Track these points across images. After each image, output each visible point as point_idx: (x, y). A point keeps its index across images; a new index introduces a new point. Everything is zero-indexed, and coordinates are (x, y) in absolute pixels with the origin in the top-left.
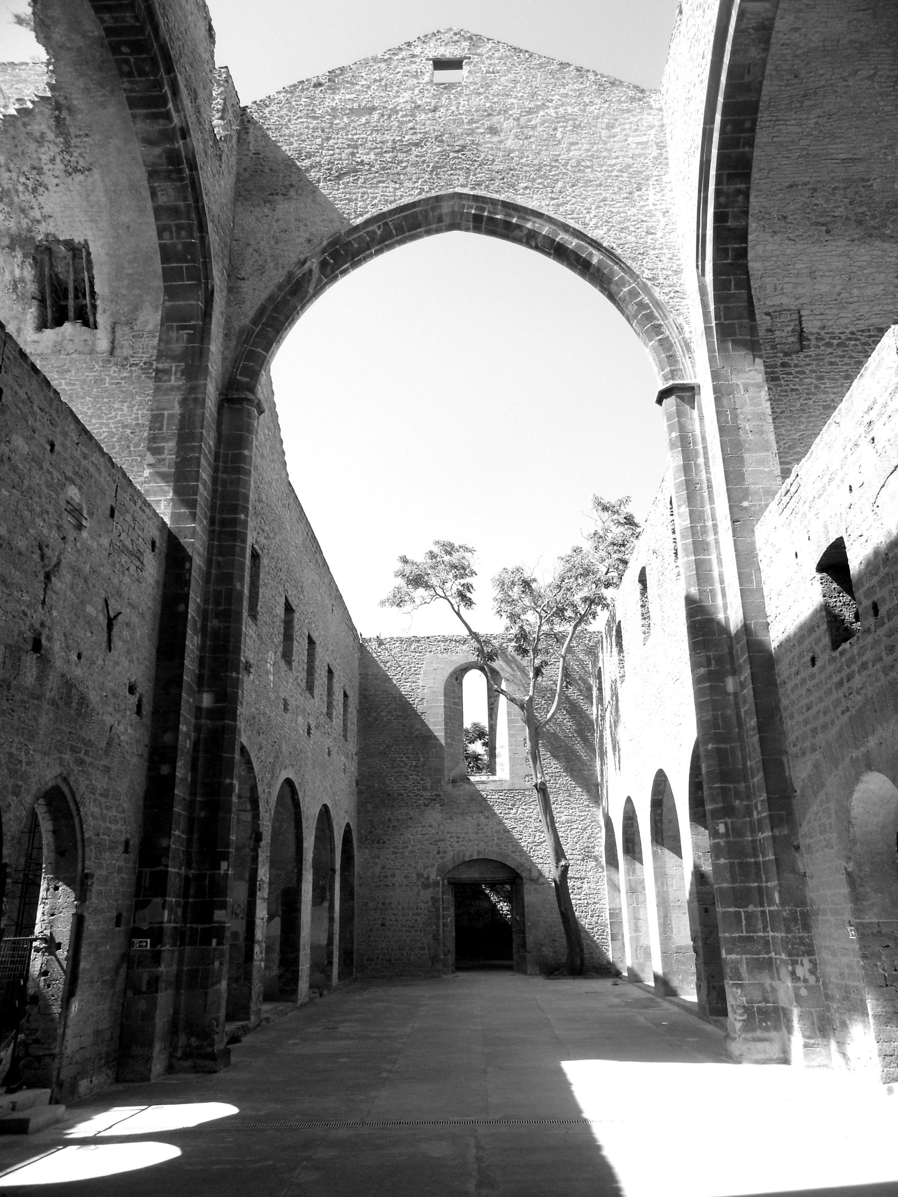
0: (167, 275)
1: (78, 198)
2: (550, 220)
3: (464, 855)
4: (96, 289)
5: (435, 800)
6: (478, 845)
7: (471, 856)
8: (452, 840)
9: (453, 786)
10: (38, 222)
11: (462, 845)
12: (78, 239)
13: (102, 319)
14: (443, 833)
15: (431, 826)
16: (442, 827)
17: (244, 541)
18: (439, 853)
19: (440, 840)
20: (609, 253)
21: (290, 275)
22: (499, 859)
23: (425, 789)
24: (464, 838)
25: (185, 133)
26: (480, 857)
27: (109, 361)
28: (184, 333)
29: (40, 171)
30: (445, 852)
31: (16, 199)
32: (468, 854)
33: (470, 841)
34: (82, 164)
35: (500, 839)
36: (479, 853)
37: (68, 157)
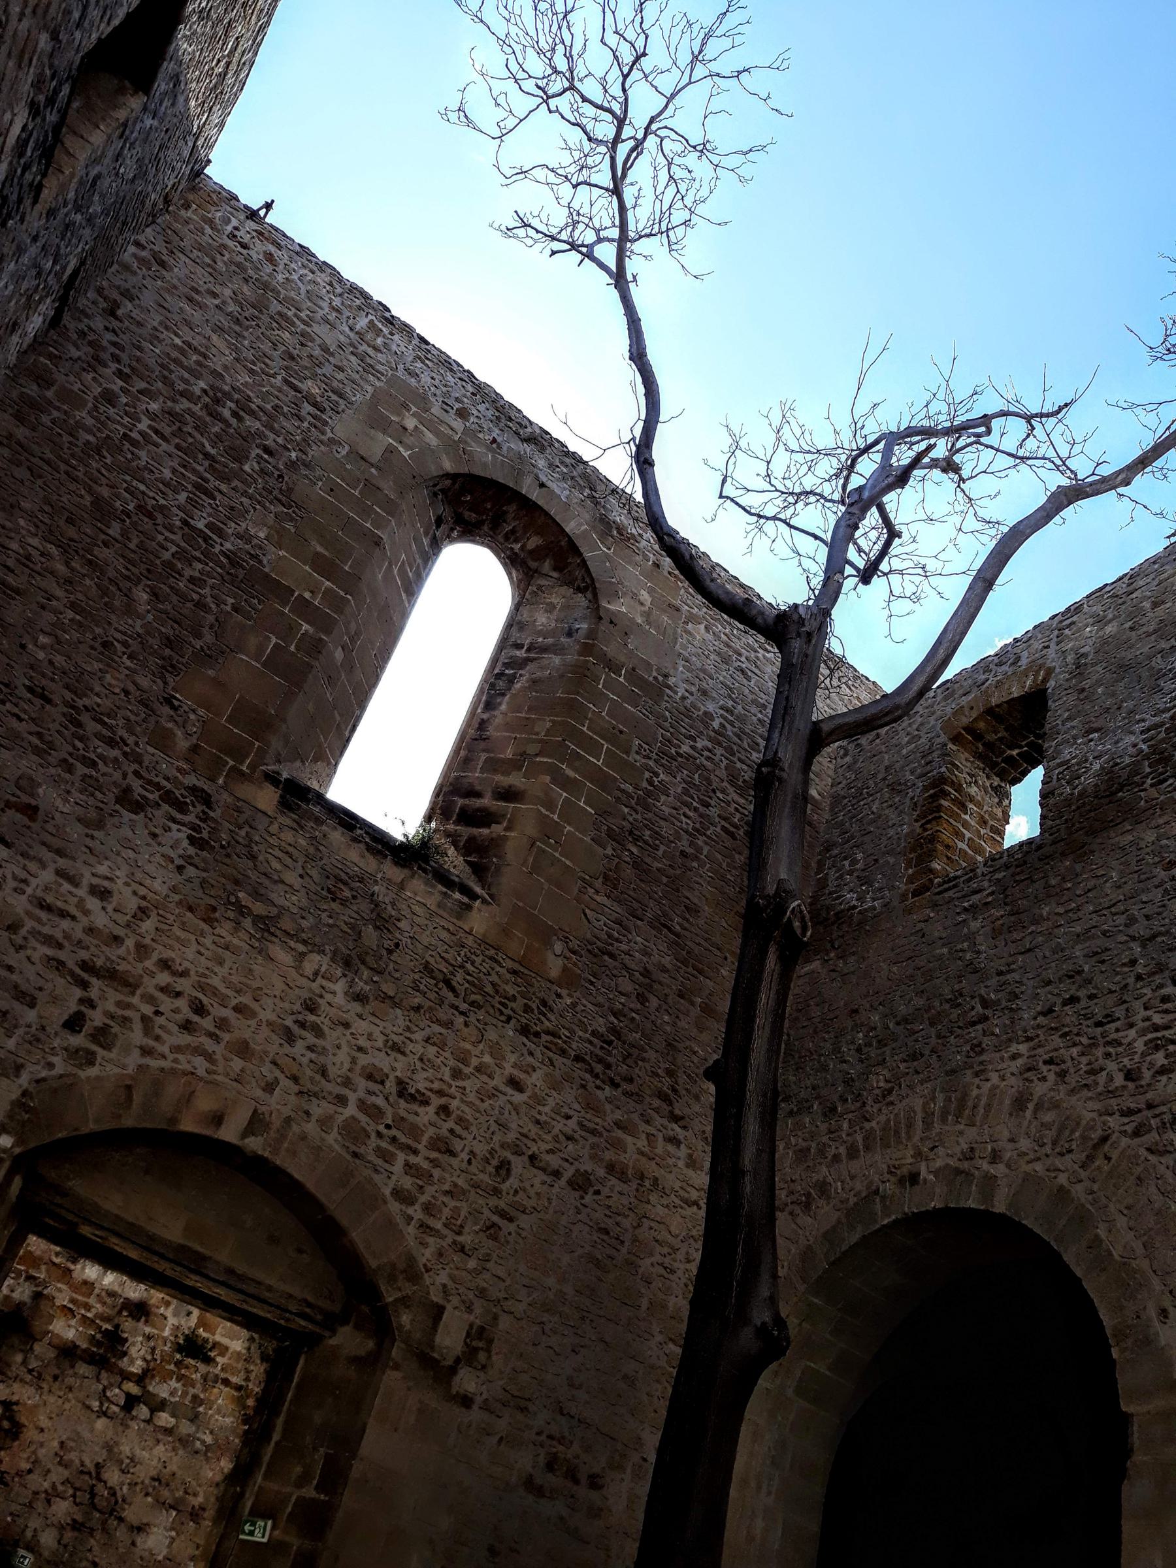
3: (188, 1098)
5: (182, 807)
6: (270, 1088)
7: (218, 1119)
8: (166, 1003)
9: (285, 805)
11: (199, 1051)
14: (142, 950)
15: (103, 894)
16: (148, 925)
18: (74, 1024)
19: (111, 975)
22: (332, 1199)
23: (162, 741)
24: (222, 1024)
26: (254, 1144)
30: (102, 1036)
32: (205, 1103)
33: (243, 1049)
35: (375, 1113)
36: (256, 1123)
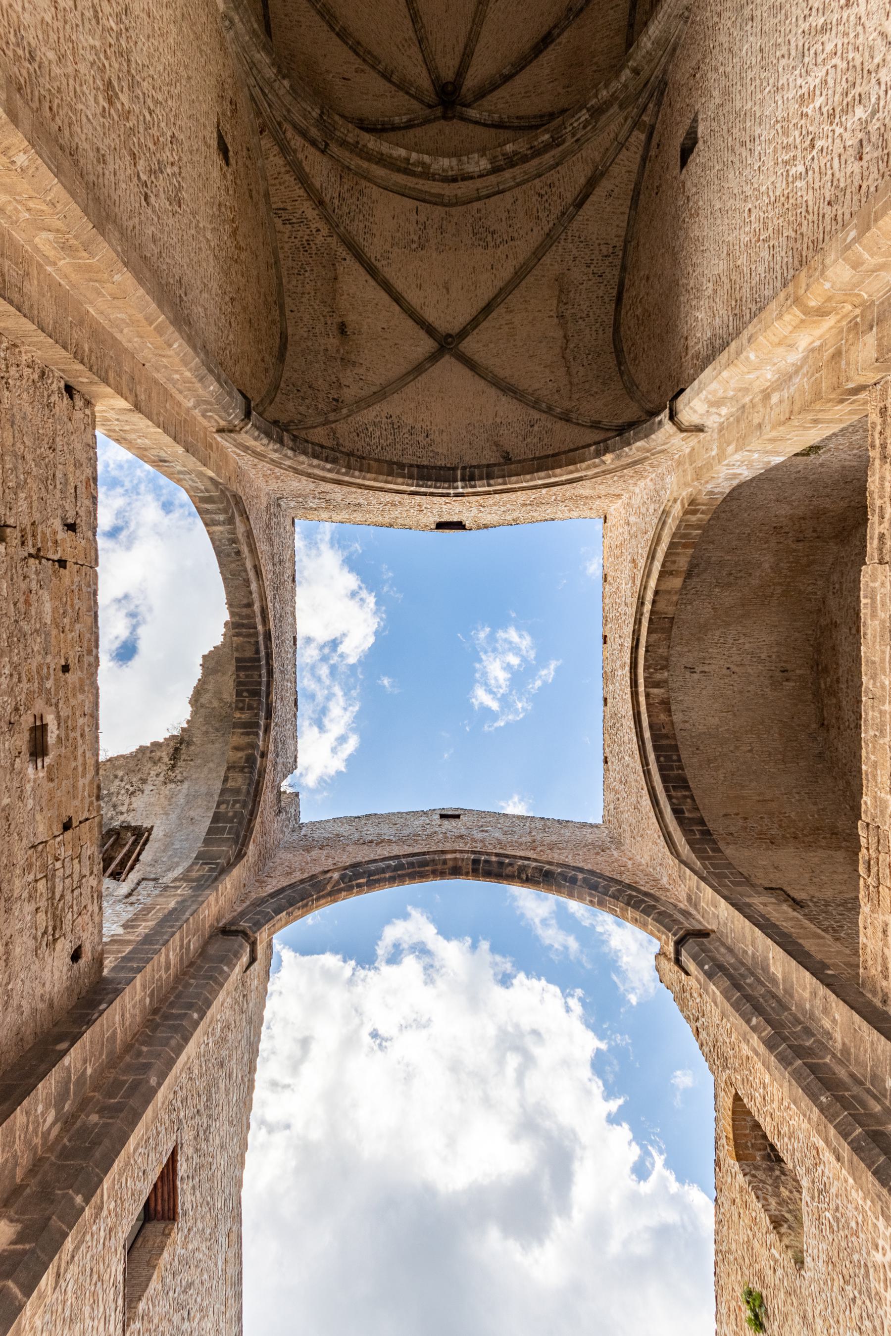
0: (210, 831)
1: (163, 800)
2: (535, 860)
4: (141, 858)
10: (122, 813)
12: (147, 824)
13: (134, 876)
17: (186, 1040)
20: (592, 872)
21: (313, 877)
25: (263, 755)
27: (120, 901)
28: (207, 867)
29: (144, 781)
31: (114, 799)
34: (179, 778)
37: (170, 773)
